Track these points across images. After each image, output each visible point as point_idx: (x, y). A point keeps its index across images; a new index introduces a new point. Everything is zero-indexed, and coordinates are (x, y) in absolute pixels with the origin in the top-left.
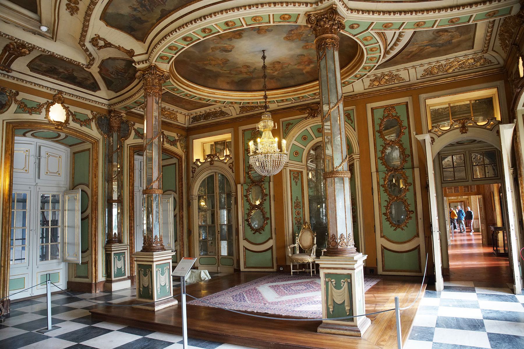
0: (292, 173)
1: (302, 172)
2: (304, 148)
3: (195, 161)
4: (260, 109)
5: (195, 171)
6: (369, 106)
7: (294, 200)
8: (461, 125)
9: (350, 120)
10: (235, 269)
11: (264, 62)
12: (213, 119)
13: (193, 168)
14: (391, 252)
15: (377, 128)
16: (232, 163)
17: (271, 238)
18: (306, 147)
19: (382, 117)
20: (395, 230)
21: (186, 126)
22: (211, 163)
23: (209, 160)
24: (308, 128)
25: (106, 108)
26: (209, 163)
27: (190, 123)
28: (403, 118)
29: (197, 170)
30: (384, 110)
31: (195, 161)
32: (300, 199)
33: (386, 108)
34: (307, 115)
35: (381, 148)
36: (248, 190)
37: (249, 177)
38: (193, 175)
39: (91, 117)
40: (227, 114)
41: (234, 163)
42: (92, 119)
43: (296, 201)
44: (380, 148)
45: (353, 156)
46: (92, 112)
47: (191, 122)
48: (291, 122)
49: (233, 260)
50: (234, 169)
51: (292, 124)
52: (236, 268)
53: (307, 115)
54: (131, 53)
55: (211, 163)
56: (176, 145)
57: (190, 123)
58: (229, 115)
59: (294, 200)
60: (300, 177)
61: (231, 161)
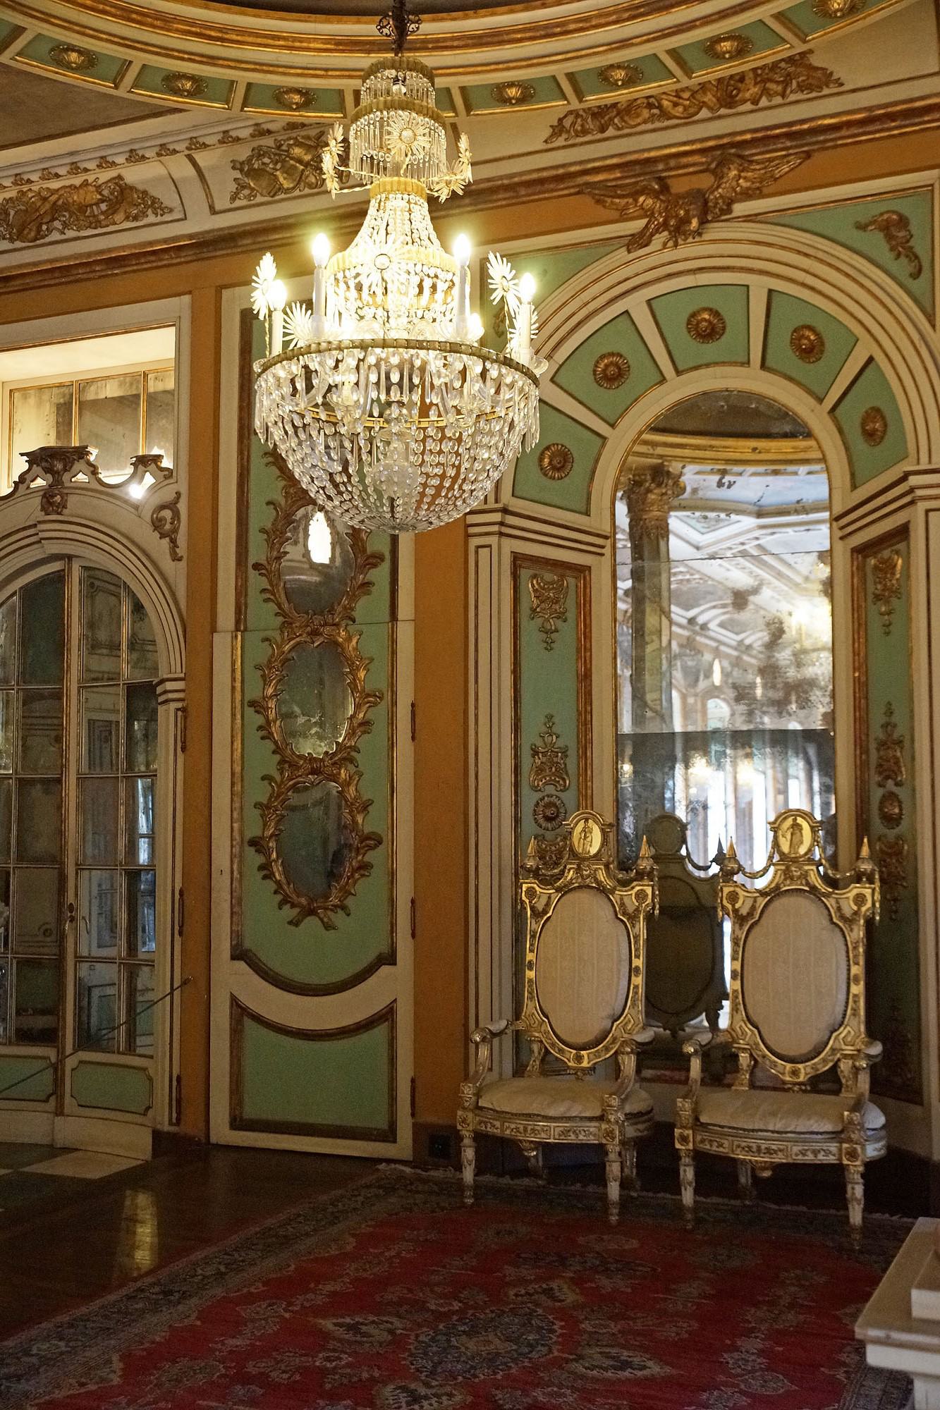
0: (525, 574)
7: (530, 736)
9: (903, 260)
10: (157, 1135)
12: (70, 234)
16: (172, 506)
18: (613, 426)
22: (52, 501)
23: (40, 482)
24: (636, 305)
26: (37, 501)
34: (637, 225)
41: (183, 506)
43: (539, 743)
49: (150, 1079)
52: (166, 1128)
55: (52, 501)
61: (168, 495)
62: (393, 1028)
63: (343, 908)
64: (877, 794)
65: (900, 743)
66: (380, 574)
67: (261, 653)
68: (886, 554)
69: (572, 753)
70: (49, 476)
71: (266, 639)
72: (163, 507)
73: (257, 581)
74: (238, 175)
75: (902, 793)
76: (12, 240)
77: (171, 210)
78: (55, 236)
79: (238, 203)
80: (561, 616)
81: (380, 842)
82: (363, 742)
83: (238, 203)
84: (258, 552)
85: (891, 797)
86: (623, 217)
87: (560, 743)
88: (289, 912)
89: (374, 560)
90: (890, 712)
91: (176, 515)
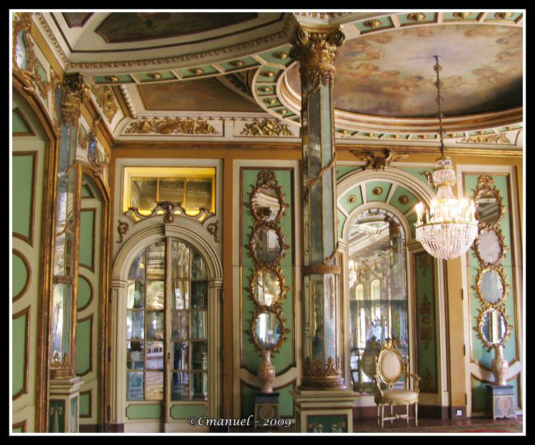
2: (347, 215)
3: (125, 209)
5: (126, 229)
11: (438, 76)
12: (179, 134)
13: (121, 224)
16: (215, 225)
17: (294, 365)
24: (363, 184)
27: (123, 133)
28: (503, 194)
29: (132, 229)
30: (479, 179)
34: (364, 163)
40: (213, 130)
41: (219, 225)
47: (125, 129)
50: (219, 234)
57: (123, 133)
58: (216, 135)
61: (213, 220)
63: (278, 352)
64: (421, 317)
67: (249, 274)
72: (213, 224)
73: (245, 251)
74: (245, 127)
77: (219, 133)
78: (174, 134)
81: (289, 331)
89: (287, 247)
90: (425, 295)
91: (216, 228)
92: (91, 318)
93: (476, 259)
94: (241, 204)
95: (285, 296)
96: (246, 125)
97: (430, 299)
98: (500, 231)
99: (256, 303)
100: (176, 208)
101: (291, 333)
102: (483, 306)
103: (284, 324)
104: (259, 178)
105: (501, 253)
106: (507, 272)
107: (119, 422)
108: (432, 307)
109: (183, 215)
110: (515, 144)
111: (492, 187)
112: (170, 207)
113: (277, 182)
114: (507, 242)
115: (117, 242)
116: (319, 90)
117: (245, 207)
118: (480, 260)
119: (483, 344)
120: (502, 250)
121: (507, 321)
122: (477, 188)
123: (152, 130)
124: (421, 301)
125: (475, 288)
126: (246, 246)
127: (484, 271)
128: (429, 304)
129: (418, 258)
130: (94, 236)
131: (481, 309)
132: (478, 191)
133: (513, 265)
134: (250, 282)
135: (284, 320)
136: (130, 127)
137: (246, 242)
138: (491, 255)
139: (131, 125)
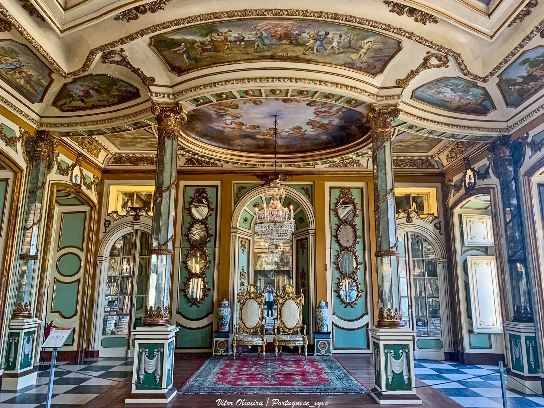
1: (249, 241)
3: (110, 212)
4: (211, 165)
5: (109, 224)
6: (327, 185)
8: (406, 215)
12: (145, 165)
13: (106, 221)
14: (343, 330)
15: (333, 207)
19: (338, 198)
20: (345, 307)
21: (102, 166)
23: (132, 214)
24: (263, 195)
25: (35, 126)
29: (113, 224)
30: (341, 191)
31: (110, 212)
32: (246, 270)
33: (343, 188)
34: (263, 182)
35: (336, 227)
36: (187, 256)
37: (188, 240)
38: (106, 229)
39: (18, 134)
42: (20, 138)
44: (334, 227)
45: (309, 231)
46: (20, 128)
47: (110, 162)
48: (245, 186)
51: (246, 188)
53: (263, 182)
54: (149, 81)
56: (91, 189)
59: (240, 270)
60: (247, 246)
62: (212, 326)
63: (202, 303)
64: (300, 282)
65: (305, 273)
66: (212, 239)
67: (186, 252)
68: (303, 241)
69: (246, 273)
70: (135, 213)
71: (186, 250)
75: (306, 282)
76: (131, 164)
79: (185, 165)
80: (245, 247)
82: (207, 270)
83: (185, 165)
84: (185, 232)
85: (303, 283)
86: (262, 180)
87: (244, 271)
88: (190, 304)
89: (212, 236)
92: (78, 280)
93: (337, 244)
94: (184, 208)
95: (208, 267)
96: (187, 159)
97: (306, 271)
98: (355, 225)
99: (190, 272)
100: (142, 211)
101: (211, 291)
102: (342, 276)
103: (206, 285)
104: (196, 193)
105: (355, 240)
106: (359, 253)
107: (96, 349)
108: (306, 276)
109: (147, 215)
110: (367, 168)
111: (350, 196)
112: (138, 211)
113: (207, 194)
114: (359, 233)
115: (103, 232)
116: (164, 143)
117: (186, 211)
118: (340, 245)
119: (341, 302)
120: (356, 239)
121: (359, 287)
122: (339, 197)
123: (128, 163)
124: (300, 271)
125: (336, 263)
126: (185, 235)
127: (342, 253)
128: (305, 273)
129: (299, 242)
130: (84, 229)
131: (340, 278)
132: (340, 199)
133: (364, 249)
134: (187, 258)
135: (207, 283)
136: (114, 160)
137: (185, 232)
138: (348, 241)
139: (114, 159)
